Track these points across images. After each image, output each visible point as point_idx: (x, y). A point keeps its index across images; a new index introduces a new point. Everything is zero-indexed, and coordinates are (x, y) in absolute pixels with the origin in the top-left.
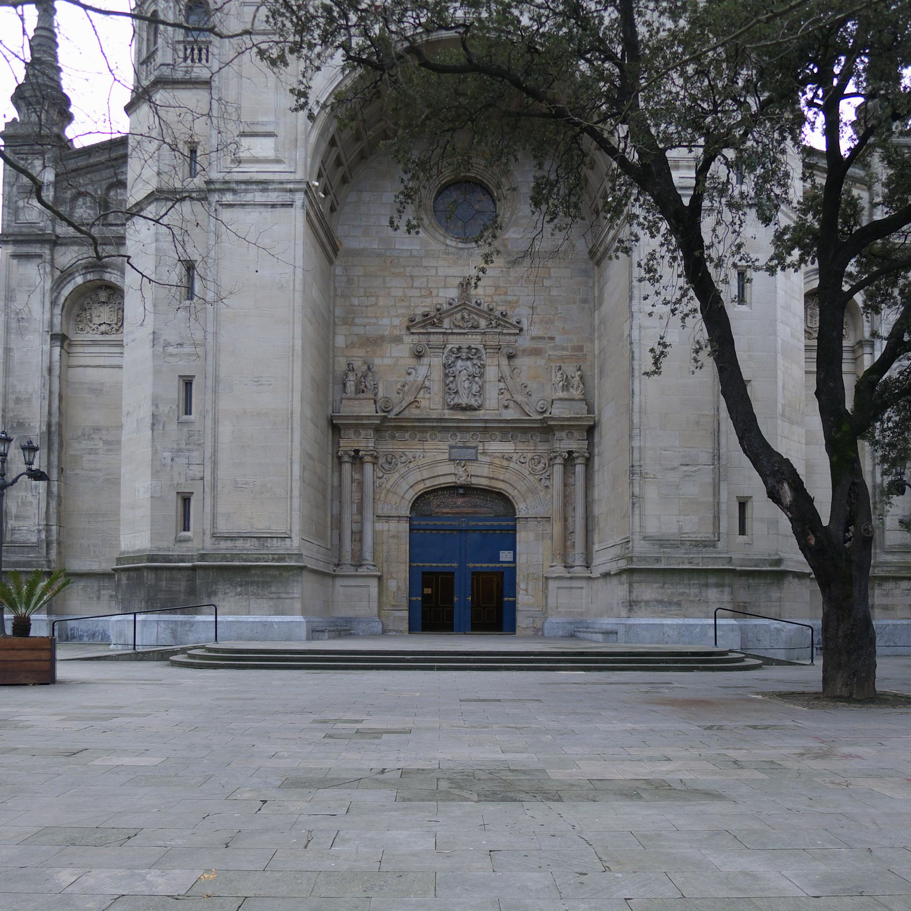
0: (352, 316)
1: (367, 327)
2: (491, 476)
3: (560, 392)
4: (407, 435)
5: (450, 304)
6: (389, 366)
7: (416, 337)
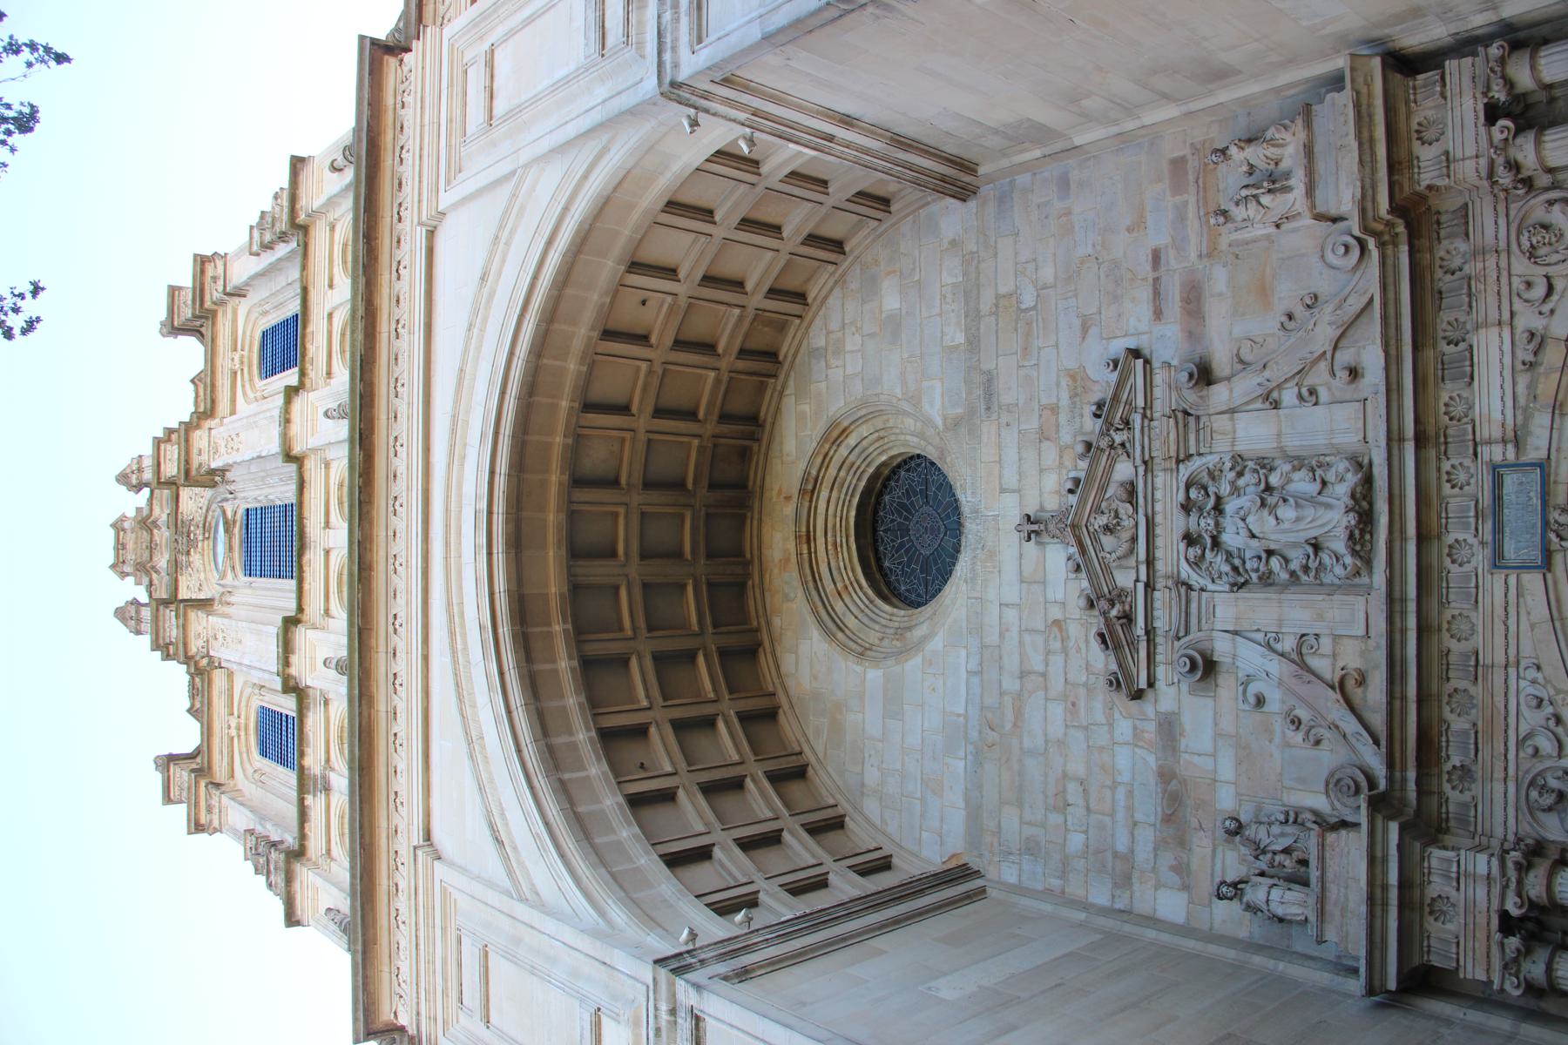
0: (1109, 855)
1: (1139, 817)
3: (1290, 197)
4: (1458, 724)
5: (1078, 569)
6: (1239, 763)
7: (1161, 672)
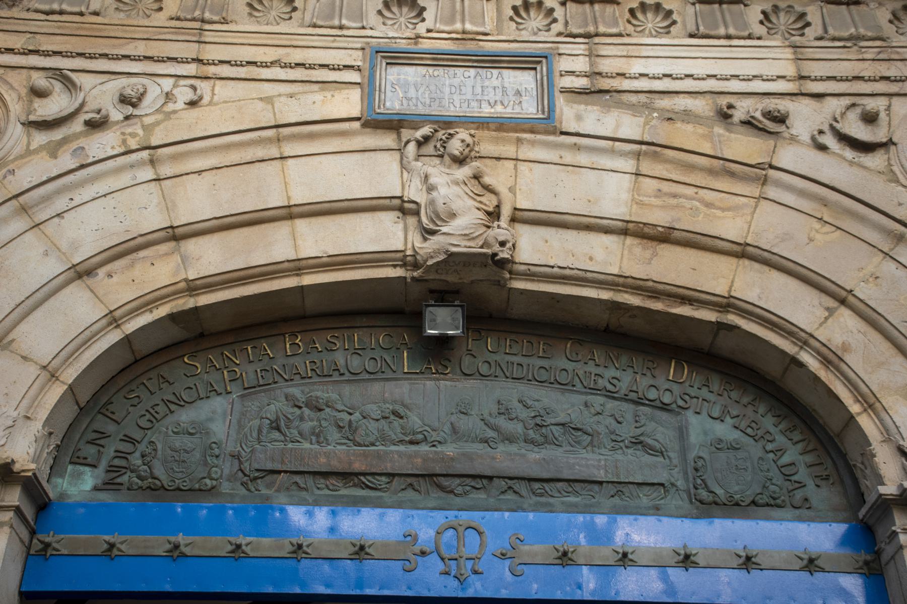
2: (659, 217)
